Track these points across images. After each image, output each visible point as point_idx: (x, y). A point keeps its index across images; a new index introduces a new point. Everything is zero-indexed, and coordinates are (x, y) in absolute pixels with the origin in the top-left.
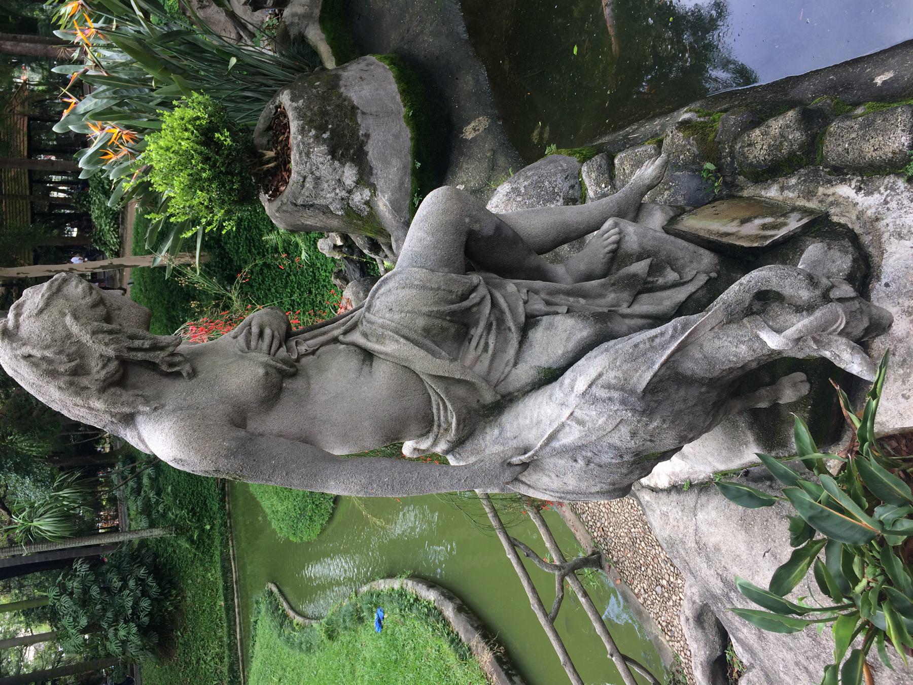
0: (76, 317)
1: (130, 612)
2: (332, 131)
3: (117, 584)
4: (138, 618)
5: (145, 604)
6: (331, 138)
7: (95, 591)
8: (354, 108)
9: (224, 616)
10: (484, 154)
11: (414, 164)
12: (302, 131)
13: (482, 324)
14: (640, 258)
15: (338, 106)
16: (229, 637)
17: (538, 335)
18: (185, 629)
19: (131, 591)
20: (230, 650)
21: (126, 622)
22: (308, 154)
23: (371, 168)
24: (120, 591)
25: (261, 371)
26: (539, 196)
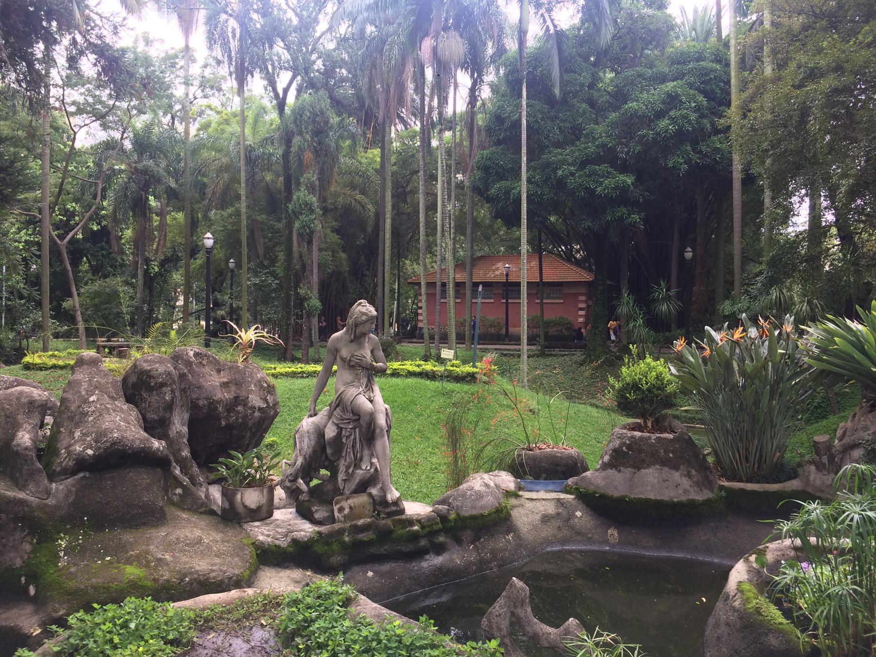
2: (627, 453)
6: (622, 451)
8: (639, 469)
12: (632, 437)
15: (643, 460)
17: (334, 428)
20: (690, 418)
22: (619, 438)
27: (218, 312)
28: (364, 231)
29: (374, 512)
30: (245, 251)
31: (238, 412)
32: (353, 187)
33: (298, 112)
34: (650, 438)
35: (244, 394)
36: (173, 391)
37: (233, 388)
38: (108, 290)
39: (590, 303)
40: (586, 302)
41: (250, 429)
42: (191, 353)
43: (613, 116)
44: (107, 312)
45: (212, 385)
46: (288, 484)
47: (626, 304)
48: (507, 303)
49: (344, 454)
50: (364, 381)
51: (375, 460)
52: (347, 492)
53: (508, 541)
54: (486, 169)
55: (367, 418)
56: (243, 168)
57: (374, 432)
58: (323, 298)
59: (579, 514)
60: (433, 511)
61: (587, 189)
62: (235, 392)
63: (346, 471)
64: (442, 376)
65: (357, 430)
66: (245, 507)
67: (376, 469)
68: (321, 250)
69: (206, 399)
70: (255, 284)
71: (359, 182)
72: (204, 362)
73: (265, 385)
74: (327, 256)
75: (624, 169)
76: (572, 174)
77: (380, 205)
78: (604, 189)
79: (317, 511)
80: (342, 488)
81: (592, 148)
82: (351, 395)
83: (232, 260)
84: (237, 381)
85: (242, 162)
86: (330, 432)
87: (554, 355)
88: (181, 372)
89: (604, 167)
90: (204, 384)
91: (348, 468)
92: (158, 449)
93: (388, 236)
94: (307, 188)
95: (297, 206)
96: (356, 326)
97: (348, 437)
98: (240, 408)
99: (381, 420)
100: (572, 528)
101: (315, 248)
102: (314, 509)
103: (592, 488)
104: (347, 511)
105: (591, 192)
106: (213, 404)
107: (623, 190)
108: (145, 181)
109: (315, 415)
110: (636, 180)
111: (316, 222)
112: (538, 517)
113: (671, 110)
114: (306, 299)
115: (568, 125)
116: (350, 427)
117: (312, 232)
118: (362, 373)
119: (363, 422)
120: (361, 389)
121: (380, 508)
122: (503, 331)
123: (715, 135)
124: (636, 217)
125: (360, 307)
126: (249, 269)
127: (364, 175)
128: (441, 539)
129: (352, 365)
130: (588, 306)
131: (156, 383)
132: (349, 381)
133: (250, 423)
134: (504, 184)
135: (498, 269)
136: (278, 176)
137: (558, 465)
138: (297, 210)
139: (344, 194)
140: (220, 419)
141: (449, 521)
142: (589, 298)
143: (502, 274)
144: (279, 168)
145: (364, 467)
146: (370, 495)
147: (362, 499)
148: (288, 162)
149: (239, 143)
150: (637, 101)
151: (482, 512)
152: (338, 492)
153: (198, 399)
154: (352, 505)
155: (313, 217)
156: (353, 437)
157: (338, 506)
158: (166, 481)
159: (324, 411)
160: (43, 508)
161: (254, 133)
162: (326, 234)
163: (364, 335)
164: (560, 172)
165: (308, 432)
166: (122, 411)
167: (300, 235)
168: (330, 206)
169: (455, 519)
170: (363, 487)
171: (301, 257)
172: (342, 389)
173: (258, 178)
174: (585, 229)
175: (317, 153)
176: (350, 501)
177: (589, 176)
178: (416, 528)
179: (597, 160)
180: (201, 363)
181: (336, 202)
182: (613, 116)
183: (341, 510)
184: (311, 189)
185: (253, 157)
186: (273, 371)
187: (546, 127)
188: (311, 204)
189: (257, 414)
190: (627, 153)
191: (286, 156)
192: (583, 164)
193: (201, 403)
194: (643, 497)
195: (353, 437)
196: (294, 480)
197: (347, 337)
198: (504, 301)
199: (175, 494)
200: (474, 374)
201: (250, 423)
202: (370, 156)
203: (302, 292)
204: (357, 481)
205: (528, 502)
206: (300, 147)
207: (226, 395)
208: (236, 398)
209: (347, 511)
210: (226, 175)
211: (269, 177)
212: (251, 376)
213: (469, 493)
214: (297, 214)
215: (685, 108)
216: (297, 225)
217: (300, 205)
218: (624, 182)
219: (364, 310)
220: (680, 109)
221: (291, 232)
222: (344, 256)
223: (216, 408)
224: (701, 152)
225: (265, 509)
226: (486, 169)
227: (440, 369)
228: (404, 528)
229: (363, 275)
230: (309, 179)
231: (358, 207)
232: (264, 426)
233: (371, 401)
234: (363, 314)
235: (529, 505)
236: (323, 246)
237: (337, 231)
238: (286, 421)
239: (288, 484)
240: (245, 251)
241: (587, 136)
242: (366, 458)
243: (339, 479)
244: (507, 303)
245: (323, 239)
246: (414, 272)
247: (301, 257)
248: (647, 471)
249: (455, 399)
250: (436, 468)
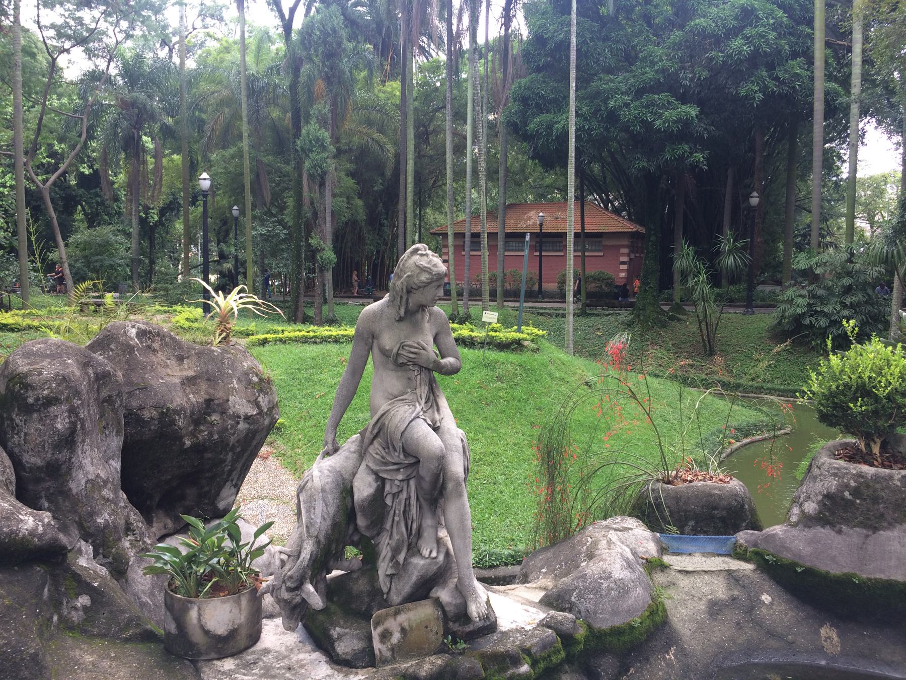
0: (408, 276)
1: (818, 309)
2: (852, 503)
3: (848, 301)
4: (812, 315)
5: (823, 322)
6: (843, 498)
7: (846, 281)
8: (875, 529)
9: (790, 387)
10: (793, 634)
11: (801, 566)
12: (860, 475)
13: (384, 454)
14: (405, 559)
15: (882, 515)
16: (768, 389)
17: (371, 479)
18: (791, 353)
19: (838, 312)
20: (756, 388)
21: (809, 305)
22: (835, 475)
23: (809, 527)
24: (841, 303)
25: (387, 348)
26: (587, 588)
27: (225, 265)
28: (383, 175)
29: (445, 636)
30: (249, 198)
31: (212, 424)
32: (369, 123)
33: (307, 32)
34: (891, 477)
35: (220, 394)
36: (72, 411)
37: (204, 386)
38: (98, 240)
39: (632, 256)
40: (628, 255)
41: (233, 449)
42: (133, 332)
43: (677, 35)
44: (98, 264)
45: (166, 385)
46: (286, 595)
47: (684, 257)
48: (541, 256)
49: (388, 526)
50: (423, 391)
51: (443, 533)
52: (396, 598)
53: (669, 665)
54: (524, 100)
55: (433, 466)
56: (244, 99)
57: (443, 487)
58: (337, 250)
59: (766, 598)
60: (543, 624)
61: (644, 123)
62: (207, 393)
63: (393, 557)
64: (482, 343)
65: (412, 483)
66: (207, 632)
67: (447, 554)
68: (334, 195)
69: (156, 407)
70: (261, 235)
71: (376, 117)
72: (156, 345)
73: (255, 379)
74: (342, 202)
75: (684, 99)
76: (627, 105)
77: (400, 145)
78: (664, 122)
79: (340, 637)
80: (385, 590)
81: (650, 74)
82: (402, 420)
83: (235, 207)
84: (211, 373)
85: (244, 93)
86: (364, 488)
87: (597, 315)
88: (100, 370)
89: (664, 97)
90: (152, 382)
91: (396, 551)
92: (33, 533)
93: (410, 179)
94: (318, 121)
95: (307, 142)
96: (409, 292)
97: (395, 496)
98: (215, 417)
99: (457, 466)
100: (758, 623)
101: (328, 194)
102: (335, 632)
103: (787, 557)
104: (396, 637)
105: (647, 125)
106: (166, 416)
107: (686, 123)
108: (137, 116)
109: (336, 450)
110: (701, 112)
111: (329, 161)
112: (702, 606)
113: (745, 27)
114: (319, 251)
115: (621, 46)
116: (400, 477)
117: (325, 173)
118: (420, 379)
119: (426, 471)
120: (419, 408)
121: (454, 627)
122: (536, 287)
123: (792, 59)
124: (699, 156)
125: (416, 258)
126: (254, 218)
127: (381, 110)
129: (402, 363)
130: (631, 259)
131: (38, 399)
132: (395, 392)
133: (232, 440)
134: (545, 117)
135: (530, 218)
136: (286, 112)
137: (715, 508)
138: (307, 146)
139: (360, 132)
140: (182, 437)
141: (577, 642)
142: (632, 251)
143: (535, 224)
144: (286, 102)
145: (426, 553)
146: (438, 603)
147: (423, 612)
148: (296, 94)
149: (239, 73)
150: (704, 16)
151: (628, 620)
152: (378, 598)
153: (141, 408)
154: (406, 625)
155: (325, 155)
156: (404, 495)
157: (380, 629)
158: (56, 585)
159: (349, 445)
161: (258, 61)
162: (339, 178)
163: (422, 307)
164: (612, 103)
165: (323, 490)
167: (311, 177)
168: (343, 147)
169: (586, 637)
170: (423, 590)
171: (312, 203)
172: (384, 407)
173: (263, 113)
174: (639, 170)
175: (328, 80)
176: (402, 618)
177: (647, 107)
178: (525, 668)
179: (656, 88)
180: (149, 347)
181: (350, 142)
182: (677, 35)
183: (385, 636)
184: (323, 122)
185: (256, 89)
186: (280, 335)
187: (595, 49)
188: (323, 140)
189: (242, 426)
190: (692, 80)
191: (293, 87)
192: (639, 93)
193: (146, 415)
194: (883, 576)
195: (404, 495)
196: (299, 587)
197: (392, 313)
198: (538, 254)
199: (75, 608)
200: (520, 340)
201: (232, 440)
202: (389, 89)
203: (313, 242)
204: (414, 578)
205: (678, 575)
206: (309, 76)
207: (195, 398)
208: (209, 402)
210: (227, 110)
211: (275, 113)
212: (233, 366)
213: (605, 585)
214: (306, 152)
215: (762, 25)
216: (307, 164)
217: (310, 141)
218: (688, 114)
219: (423, 262)
220: (756, 26)
221: (300, 176)
222: (360, 203)
223: (173, 422)
224: (777, 79)
225: (244, 632)
226: (524, 100)
227: (479, 334)
228: (504, 669)
229: (382, 225)
230: (320, 111)
231: (376, 147)
232: (255, 443)
233: (436, 429)
234: (423, 269)
235: (684, 582)
236: (337, 191)
237: (352, 175)
238: (296, 398)
239: (286, 595)
240: (249, 198)
241: (644, 59)
242: (428, 534)
243: (381, 573)
244: (541, 256)
245: (336, 183)
246: (436, 223)
247: (312, 203)
248: (889, 533)
249: (499, 372)
250: (480, 459)
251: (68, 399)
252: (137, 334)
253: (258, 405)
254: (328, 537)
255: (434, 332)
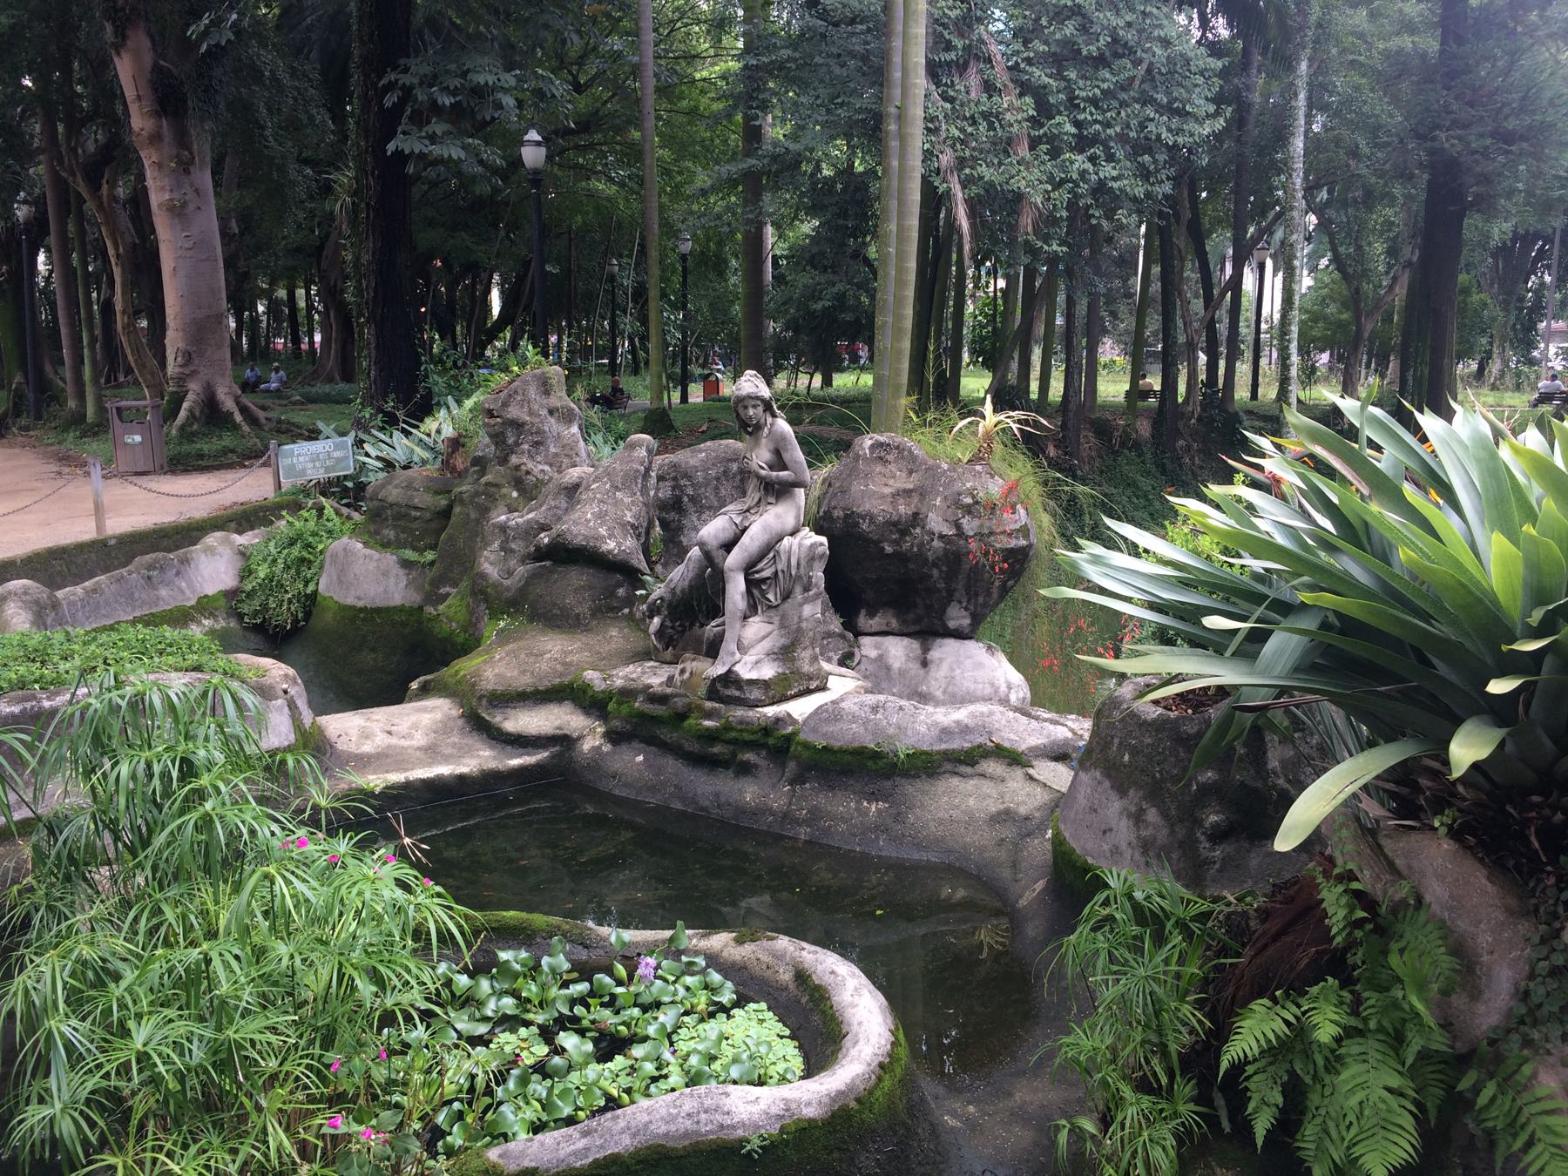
92: (610, 552)
98: (918, 530)
104: (687, 675)
128: (749, 756)
160: (496, 586)
166: (617, 503)
189: (936, 543)
193: (836, 513)
208: (916, 515)
209: (687, 675)
251: (675, 479)
252: (872, 447)
253: (958, 526)
254: (683, 591)
255: (771, 446)
